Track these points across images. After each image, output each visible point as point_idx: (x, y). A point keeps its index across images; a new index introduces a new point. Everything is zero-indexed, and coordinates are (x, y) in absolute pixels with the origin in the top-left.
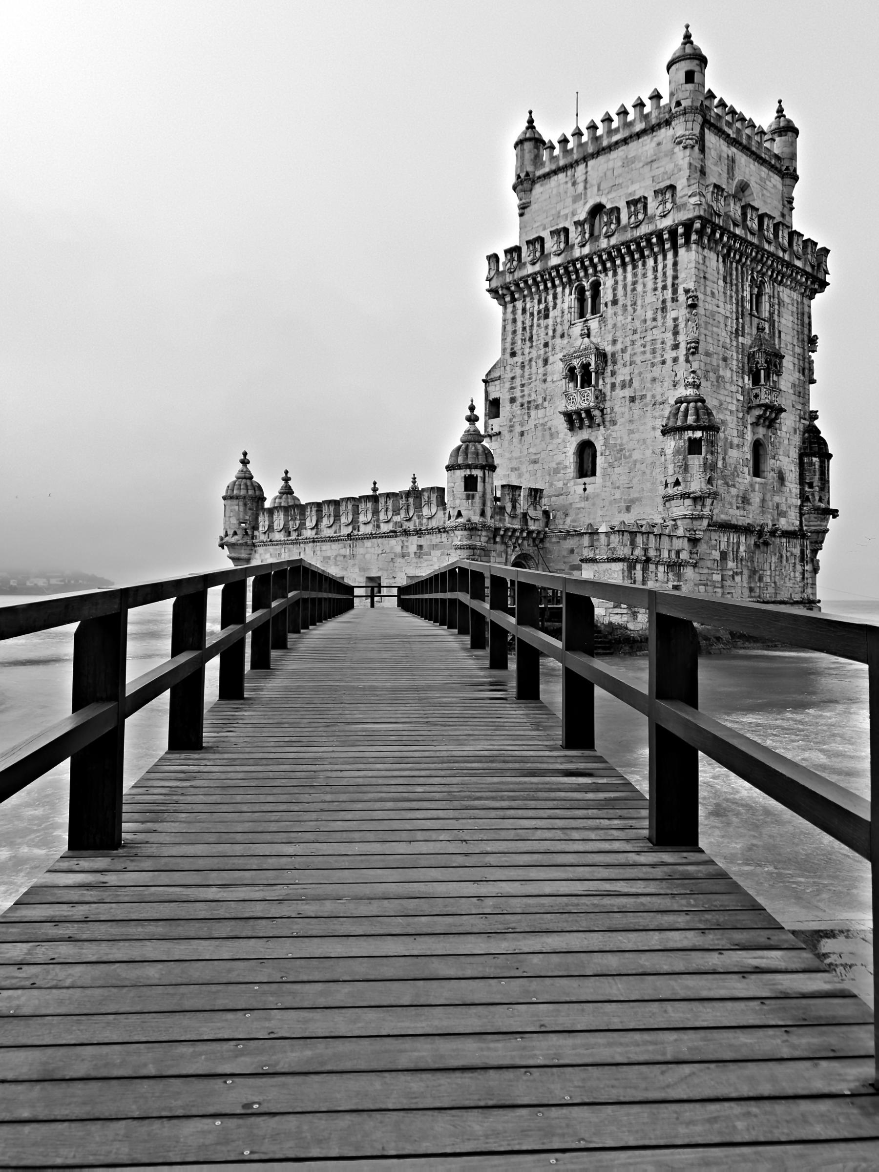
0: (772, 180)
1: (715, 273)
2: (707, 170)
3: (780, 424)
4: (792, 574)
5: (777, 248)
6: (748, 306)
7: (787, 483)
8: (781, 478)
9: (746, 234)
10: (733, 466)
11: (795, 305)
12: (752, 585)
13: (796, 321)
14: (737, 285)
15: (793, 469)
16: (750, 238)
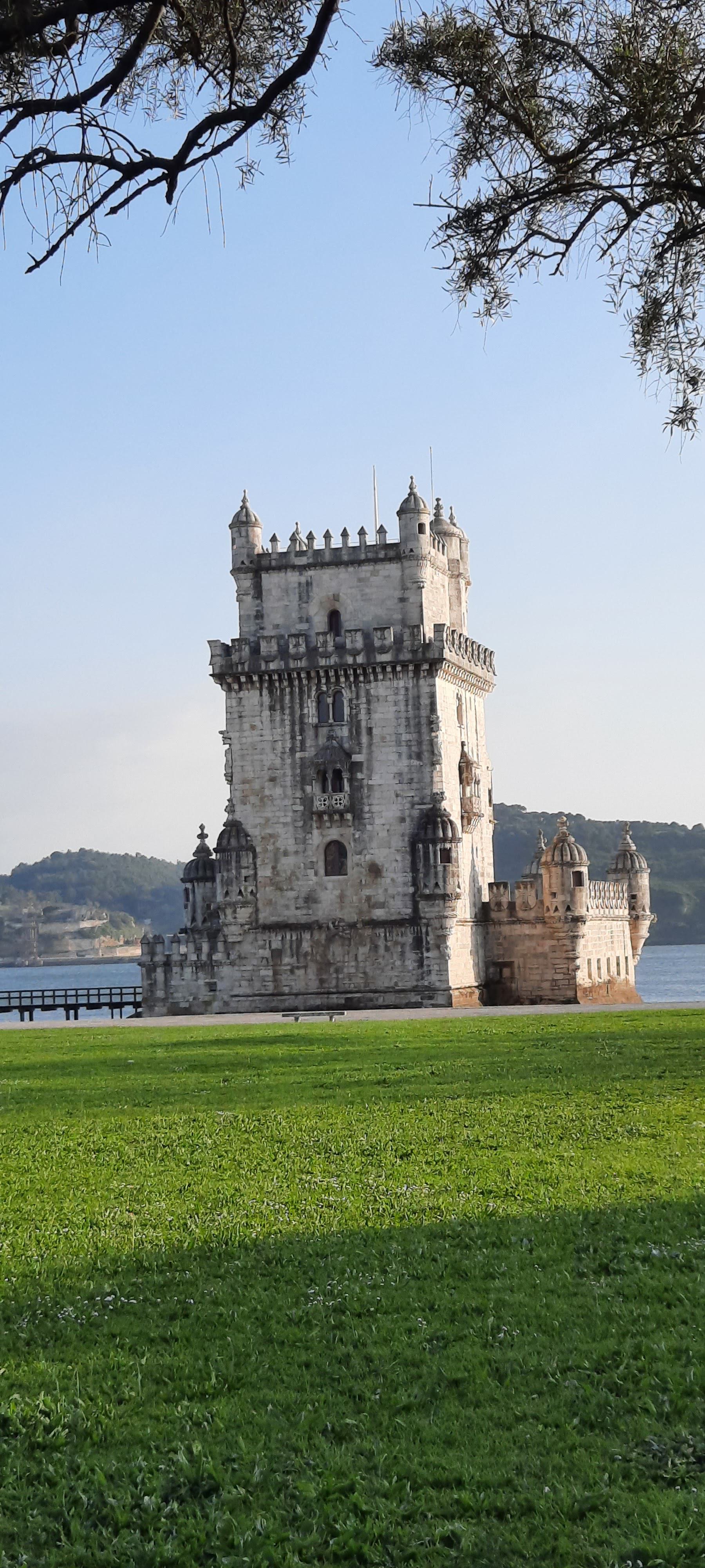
0: (383, 573)
1: (258, 708)
2: (264, 612)
3: (372, 818)
5: (341, 657)
6: (313, 720)
7: (384, 874)
8: (375, 871)
9: (287, 664)
10: (289, 873)
11: (402, 692)
12: (324, 977)
13: (403, 708)
14: (292, 708)
15: (399, 858)
16: (292, 664)
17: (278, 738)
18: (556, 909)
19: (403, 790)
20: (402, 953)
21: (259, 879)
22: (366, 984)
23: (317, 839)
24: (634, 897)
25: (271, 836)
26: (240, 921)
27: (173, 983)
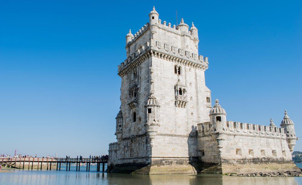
0: (147, 34)
3: (140, 103)
4: (143, 148)
7: (141, 120)
8: (140, 119)
11: (146, 64)
12: (131, 153)
15: (144, 114)
17: (127, 86)
18: (212, 131)
19: (145, 93)
20: (144, 145)
21: (123, 126)
22: (137, 155)
23: (131, 112)
24: (288, 132)
25: (126, 113)
26: (118, 138)
27: (112, 156)
